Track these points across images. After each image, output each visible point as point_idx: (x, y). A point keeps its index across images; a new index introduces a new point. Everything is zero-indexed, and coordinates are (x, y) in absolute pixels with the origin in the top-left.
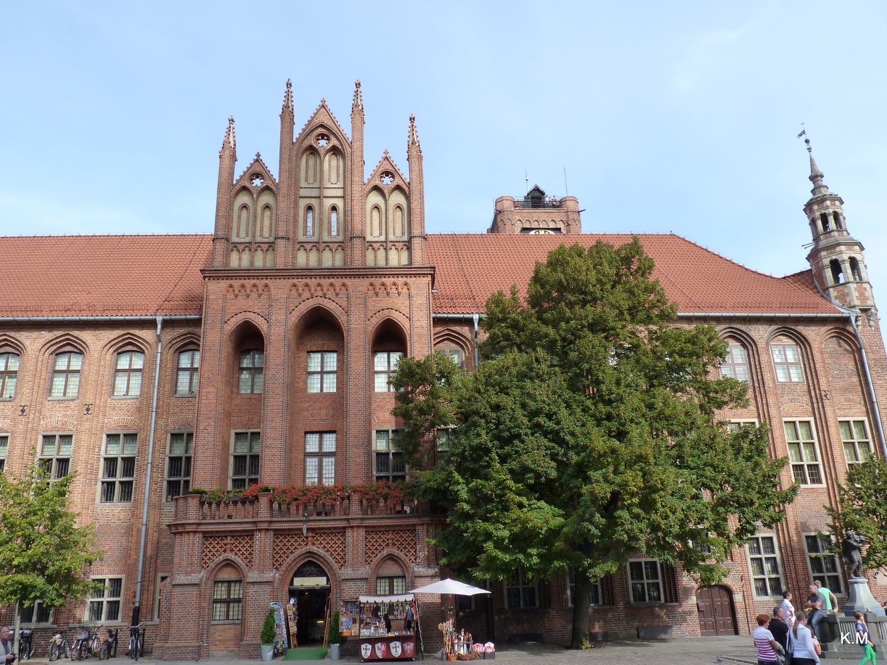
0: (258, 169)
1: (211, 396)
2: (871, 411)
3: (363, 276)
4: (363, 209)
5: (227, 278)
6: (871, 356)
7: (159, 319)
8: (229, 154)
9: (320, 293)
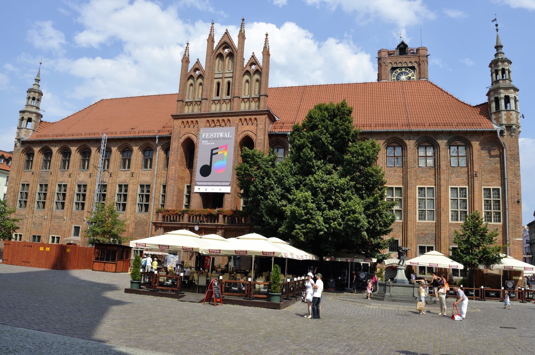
0: (197, 66)
1: (173, 170)
2: (503, 185)
3: (237, 116)
4: (240, 83)
5: (182, 118)
6: (509, 153)
7: (157, 137)
8: (186, 60)
9: (219, 124)
